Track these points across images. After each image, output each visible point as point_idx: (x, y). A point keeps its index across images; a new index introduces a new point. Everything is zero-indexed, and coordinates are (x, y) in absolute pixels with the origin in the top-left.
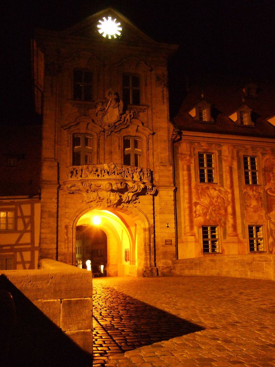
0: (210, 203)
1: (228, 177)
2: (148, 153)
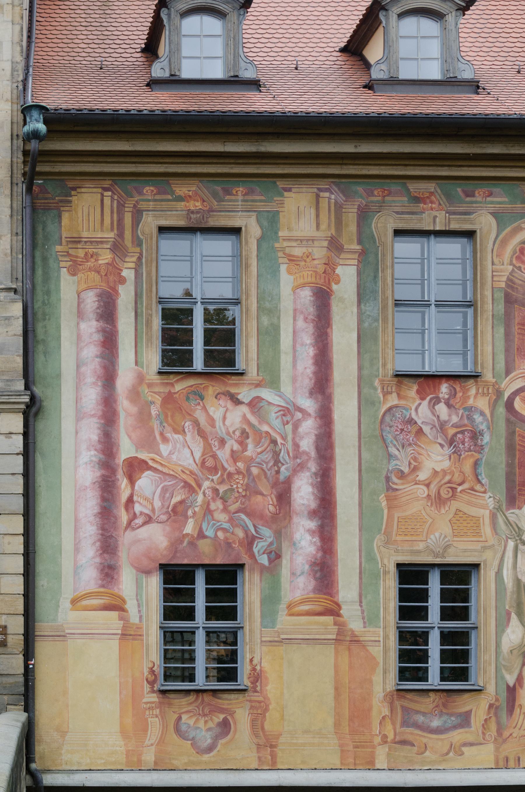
0: (203, 462)
1: (307, 339)
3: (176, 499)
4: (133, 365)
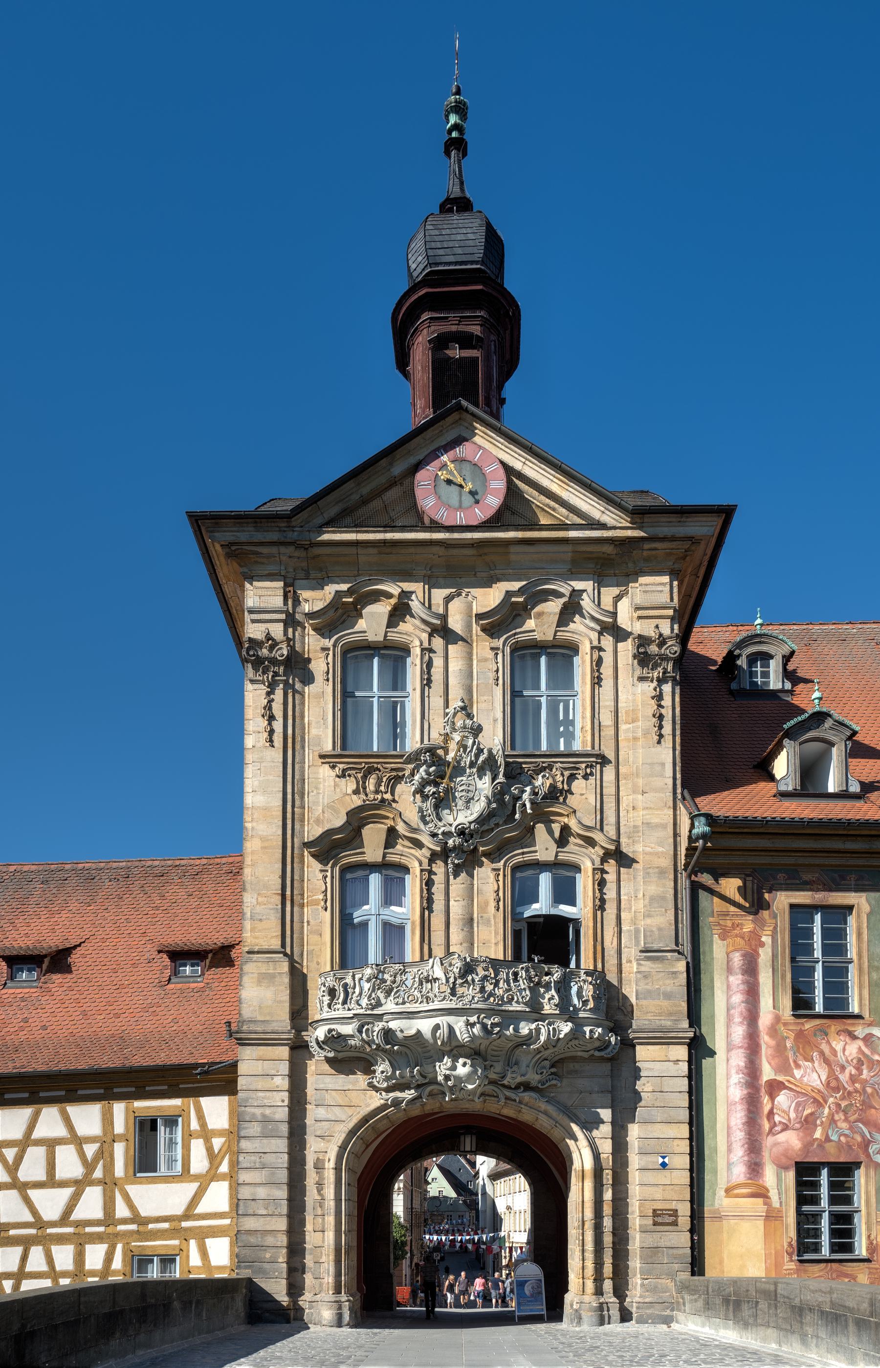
0: (828, 1083)
2: (599, 919)
3: (807, 1112)
4: (772, 1009)
